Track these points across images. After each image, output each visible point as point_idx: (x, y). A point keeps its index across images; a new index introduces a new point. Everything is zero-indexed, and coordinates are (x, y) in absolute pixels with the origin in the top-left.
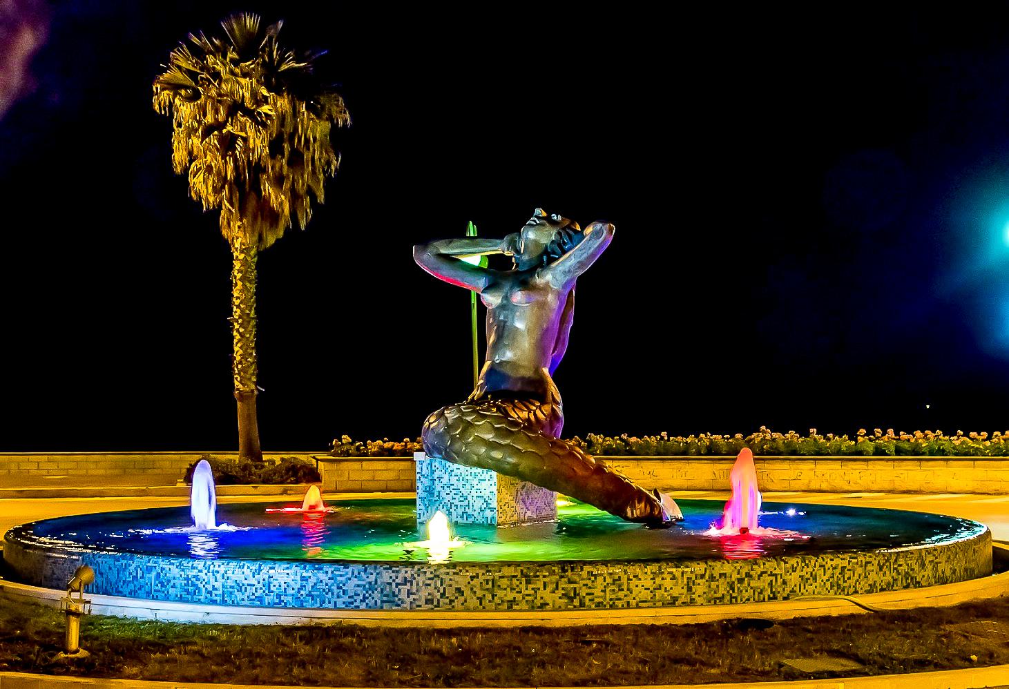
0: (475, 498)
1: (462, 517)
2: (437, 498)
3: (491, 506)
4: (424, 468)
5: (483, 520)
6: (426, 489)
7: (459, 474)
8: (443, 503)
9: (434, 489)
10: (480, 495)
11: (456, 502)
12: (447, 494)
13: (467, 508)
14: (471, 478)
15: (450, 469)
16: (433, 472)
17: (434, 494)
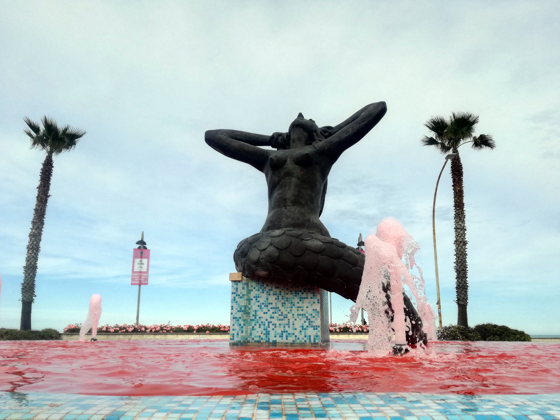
0: (296, 316)
1: (281, 336)
2: (253, 318)
3: (314, 324)
5: (305, 339)
6: (241, 309)
8: (260, 322)
9: (250, 309)
11: (274, 321)
12: (264, 313)
13: (287, 326)
14: (292, 296)
16: (249, 292)
17: (249, 313)
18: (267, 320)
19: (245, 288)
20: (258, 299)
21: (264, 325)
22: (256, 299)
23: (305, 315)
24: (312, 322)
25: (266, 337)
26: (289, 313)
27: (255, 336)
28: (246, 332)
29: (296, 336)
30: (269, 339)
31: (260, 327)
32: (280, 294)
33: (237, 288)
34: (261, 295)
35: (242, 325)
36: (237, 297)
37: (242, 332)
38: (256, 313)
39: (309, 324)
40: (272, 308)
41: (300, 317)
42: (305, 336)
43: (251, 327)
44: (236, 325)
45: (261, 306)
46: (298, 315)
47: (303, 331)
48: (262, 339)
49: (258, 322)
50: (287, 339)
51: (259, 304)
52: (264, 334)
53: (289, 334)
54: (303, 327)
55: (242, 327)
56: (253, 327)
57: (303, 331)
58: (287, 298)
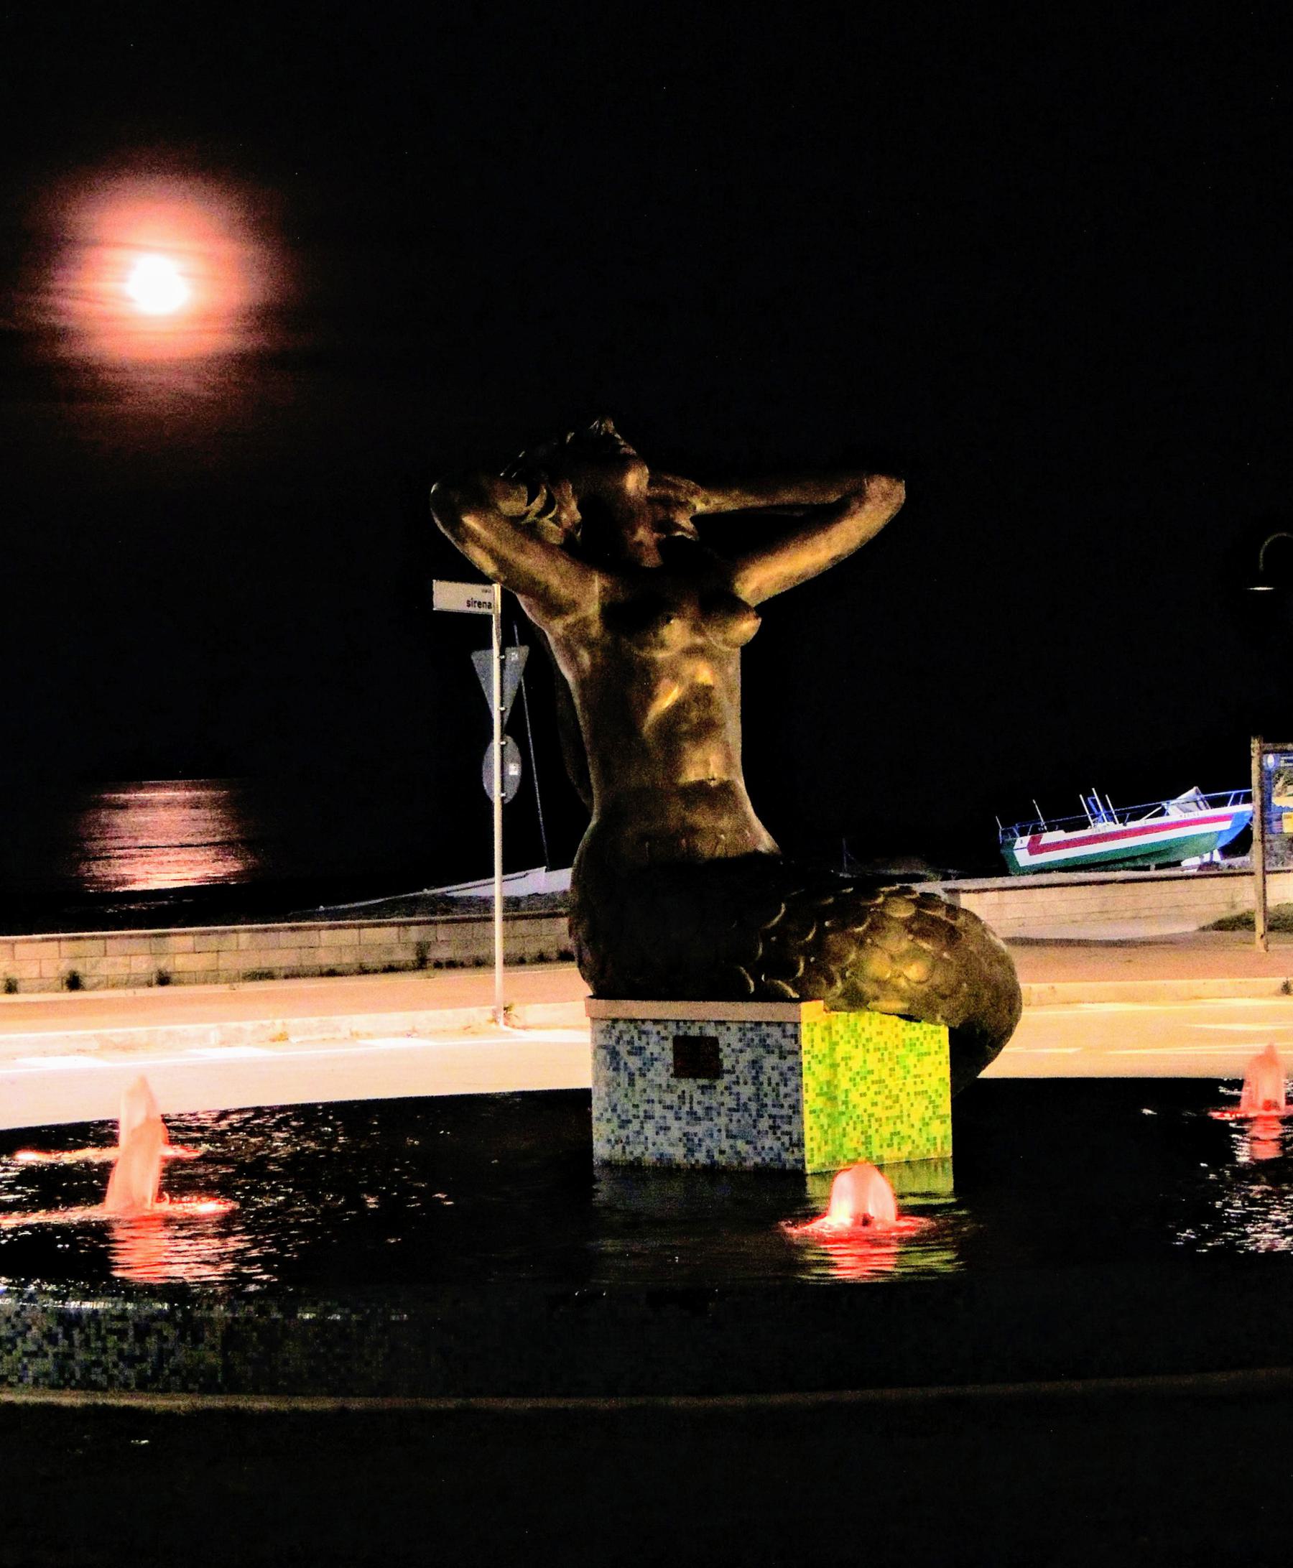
2: (843, 1108)
4: (818, 1040)
7: (882, 1045)
8: (855, 1118)
9: (836, 1086)
10: (920, 1088)
11: (878, 1111)
15: (865, 1035)
16: (833, 1046)
17: (835, 1098)
18: (865, 1111)
19: (827, 1040)
20: (850, 1063)
21: (862, 1121)
22: (846, 1064)
23: (926, 1092)
24: (937, 1107)
25: (867, 1148)
26: (901, 1090)
27: (849, 1150)
28: (834, 1141)
29: (913, 1142)
30: (871, 1153)
31: (855, 1129)
32: (886, 1049)
33: (813, 1041)
34: (854, 1053)
35: (826, 1127)
36: (813, 1062)
37: (826, 1143)
38: (847, 1097)
39: (934, 1113)
40: (873, 1082)
41: (919, 1097)
42: (928, 1140)
43: (841, 1130)
44: (815, 1129)
45: (855, 1079)
46: (916, 1093)
47: (924, 1129)
48: (859, 1155)
49: (851, 1117)
50: (899, 1149)
51: (850, 1074)
52: (863, 1143)
53: (903, 1137)
54: (924, 1119)
55: (826, 1132)
56: (844, 1129)
57: (924, 1129)
58: (897, 1057)
